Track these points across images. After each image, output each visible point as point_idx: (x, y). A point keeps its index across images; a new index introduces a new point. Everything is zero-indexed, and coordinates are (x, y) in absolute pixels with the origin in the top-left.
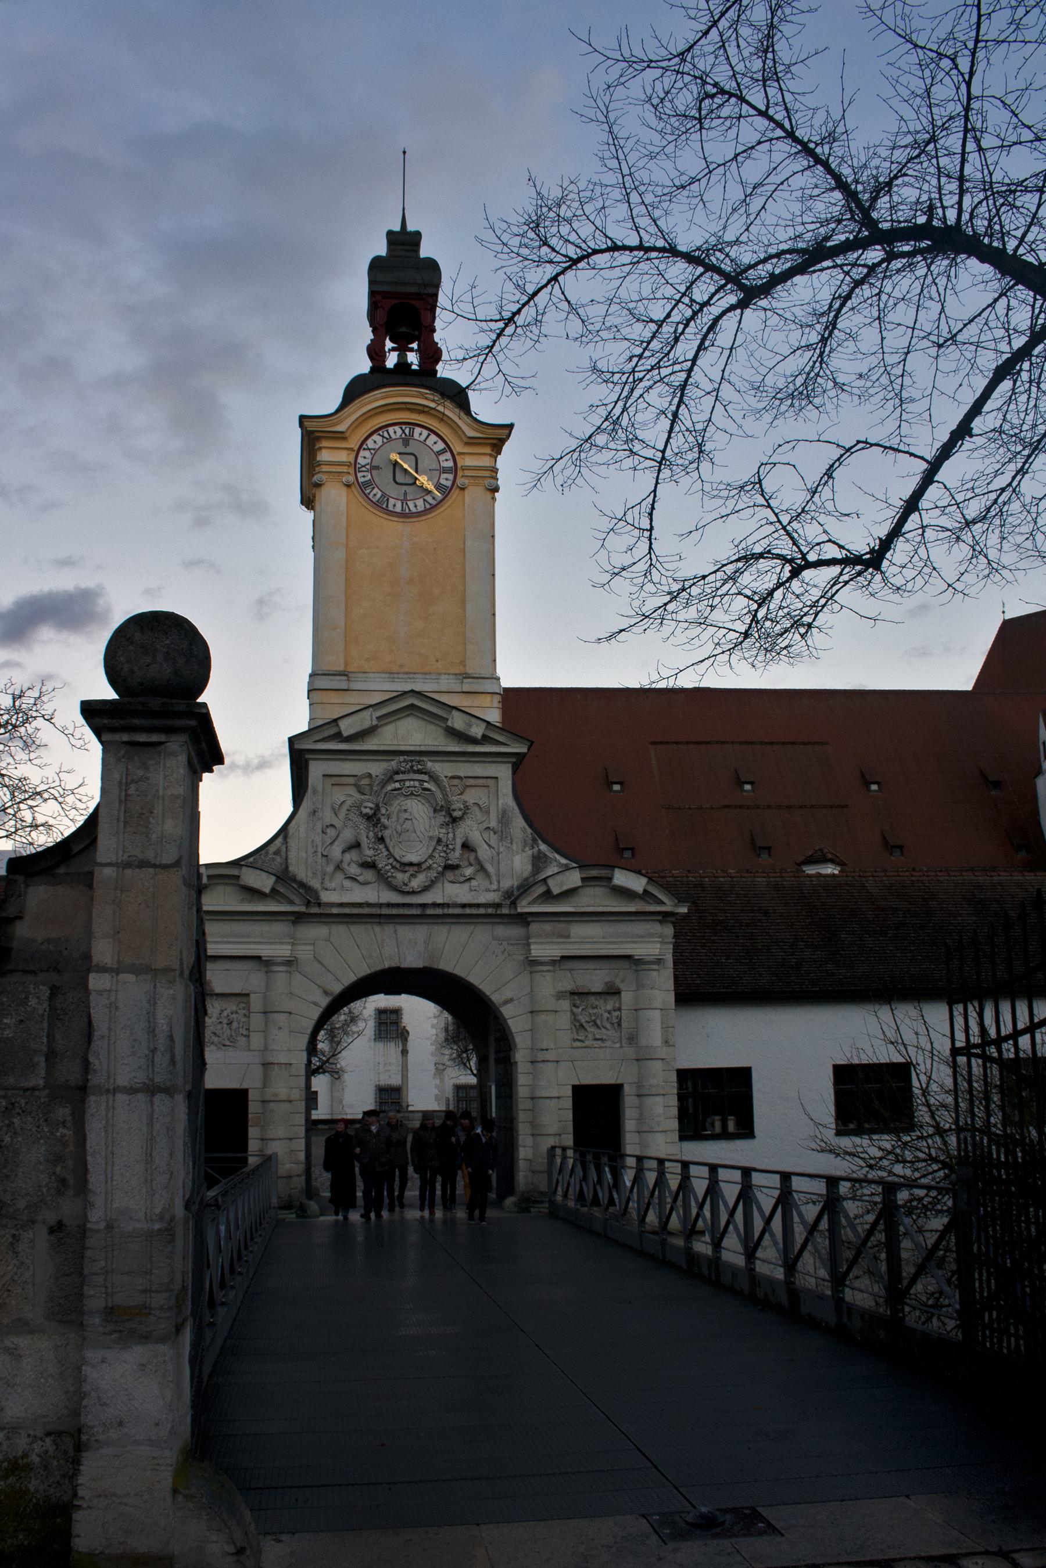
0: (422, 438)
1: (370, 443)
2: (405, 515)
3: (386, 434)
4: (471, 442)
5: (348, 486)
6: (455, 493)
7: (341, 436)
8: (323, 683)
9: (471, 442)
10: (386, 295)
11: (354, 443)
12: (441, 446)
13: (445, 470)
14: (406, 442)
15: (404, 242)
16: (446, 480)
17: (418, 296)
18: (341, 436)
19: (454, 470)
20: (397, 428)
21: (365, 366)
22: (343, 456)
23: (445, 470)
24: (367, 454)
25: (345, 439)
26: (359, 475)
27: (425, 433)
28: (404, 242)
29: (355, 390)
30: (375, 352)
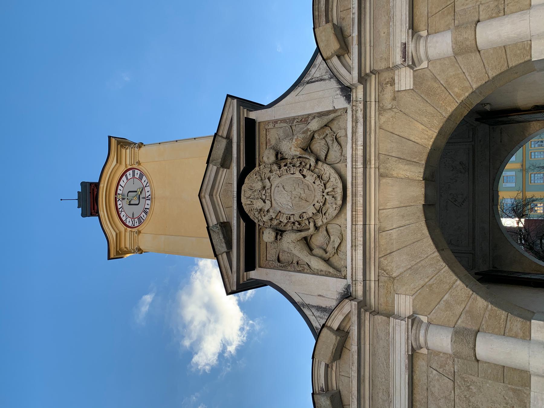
0: (122, 189)
1: (124, 219)
3: (120, 210)
5: (139, 232)
7: (118, 235)
9: (119, 161)
11: (122, 227)
18: (118, 235)
20: (118, 203)
22: (128, 234)
24: (128, 220)
25: (120, 233)
26: (136, 225)
27: (120, 187)
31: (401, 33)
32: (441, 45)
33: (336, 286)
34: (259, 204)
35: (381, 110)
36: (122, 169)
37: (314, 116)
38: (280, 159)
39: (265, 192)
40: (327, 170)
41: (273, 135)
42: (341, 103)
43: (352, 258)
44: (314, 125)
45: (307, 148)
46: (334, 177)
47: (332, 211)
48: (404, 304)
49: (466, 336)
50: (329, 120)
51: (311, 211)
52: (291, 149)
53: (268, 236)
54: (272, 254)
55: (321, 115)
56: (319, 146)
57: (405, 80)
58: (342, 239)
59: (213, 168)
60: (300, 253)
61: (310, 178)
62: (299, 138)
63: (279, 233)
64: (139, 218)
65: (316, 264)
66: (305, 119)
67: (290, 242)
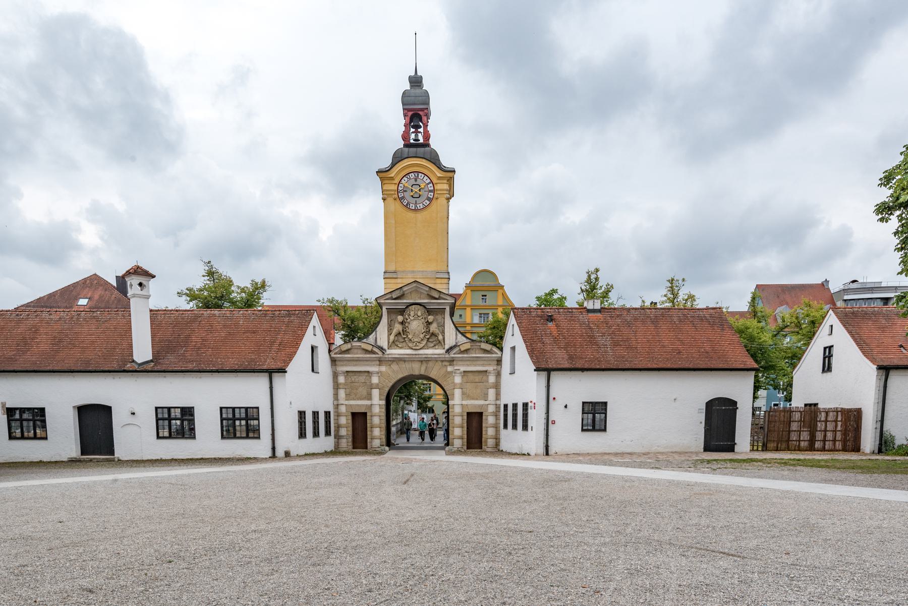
2: (416, 210)
4: (439, 178)
6: (434, 200)
8: (387, 275)
10: (409, 110)
11: (397, 181)
12: (429, 181)
13: (430, 191)
14: (416, 180)
15: (416, 81)
16: (431, 195)
17: (422, 110)
18: (392, 178)
19: (433, 191)
21: (401, 143)
23: (430, 191)
28: (416, 81)
29: (398, 158)
30: (405, 137)
31: (463, 369)
32: (458, 379)
33: (385, 346)
34: (412, 313)
35: (442, 361)
36: (435, 181)
37: (444, 336)
38: (429, 324)
39: (417, 317)
40: (424, 342)
41: (439, 317)
42: (447, 347)
43: (396, 352)
44: (440, 337)
45: (433, 334)
46: (422, 345)
47: (410, 345)
48: (383, 369)
49: (377, 386)
50: (440, 343)
51: (410, 336)
52: (433, 328)
53: (400, 318)
54: (393, 317)
55: (444, 339)
56: (433, 339)
57: (450, 369)
58: (401, 348)
59: (427, 289)
60: (395, 331)
61: (422, 336)
62: (437, 331)
63: (402, 323)
64: (403, 198)
65: (392, 337)
66: (443, 332)
67: (398, 328)
